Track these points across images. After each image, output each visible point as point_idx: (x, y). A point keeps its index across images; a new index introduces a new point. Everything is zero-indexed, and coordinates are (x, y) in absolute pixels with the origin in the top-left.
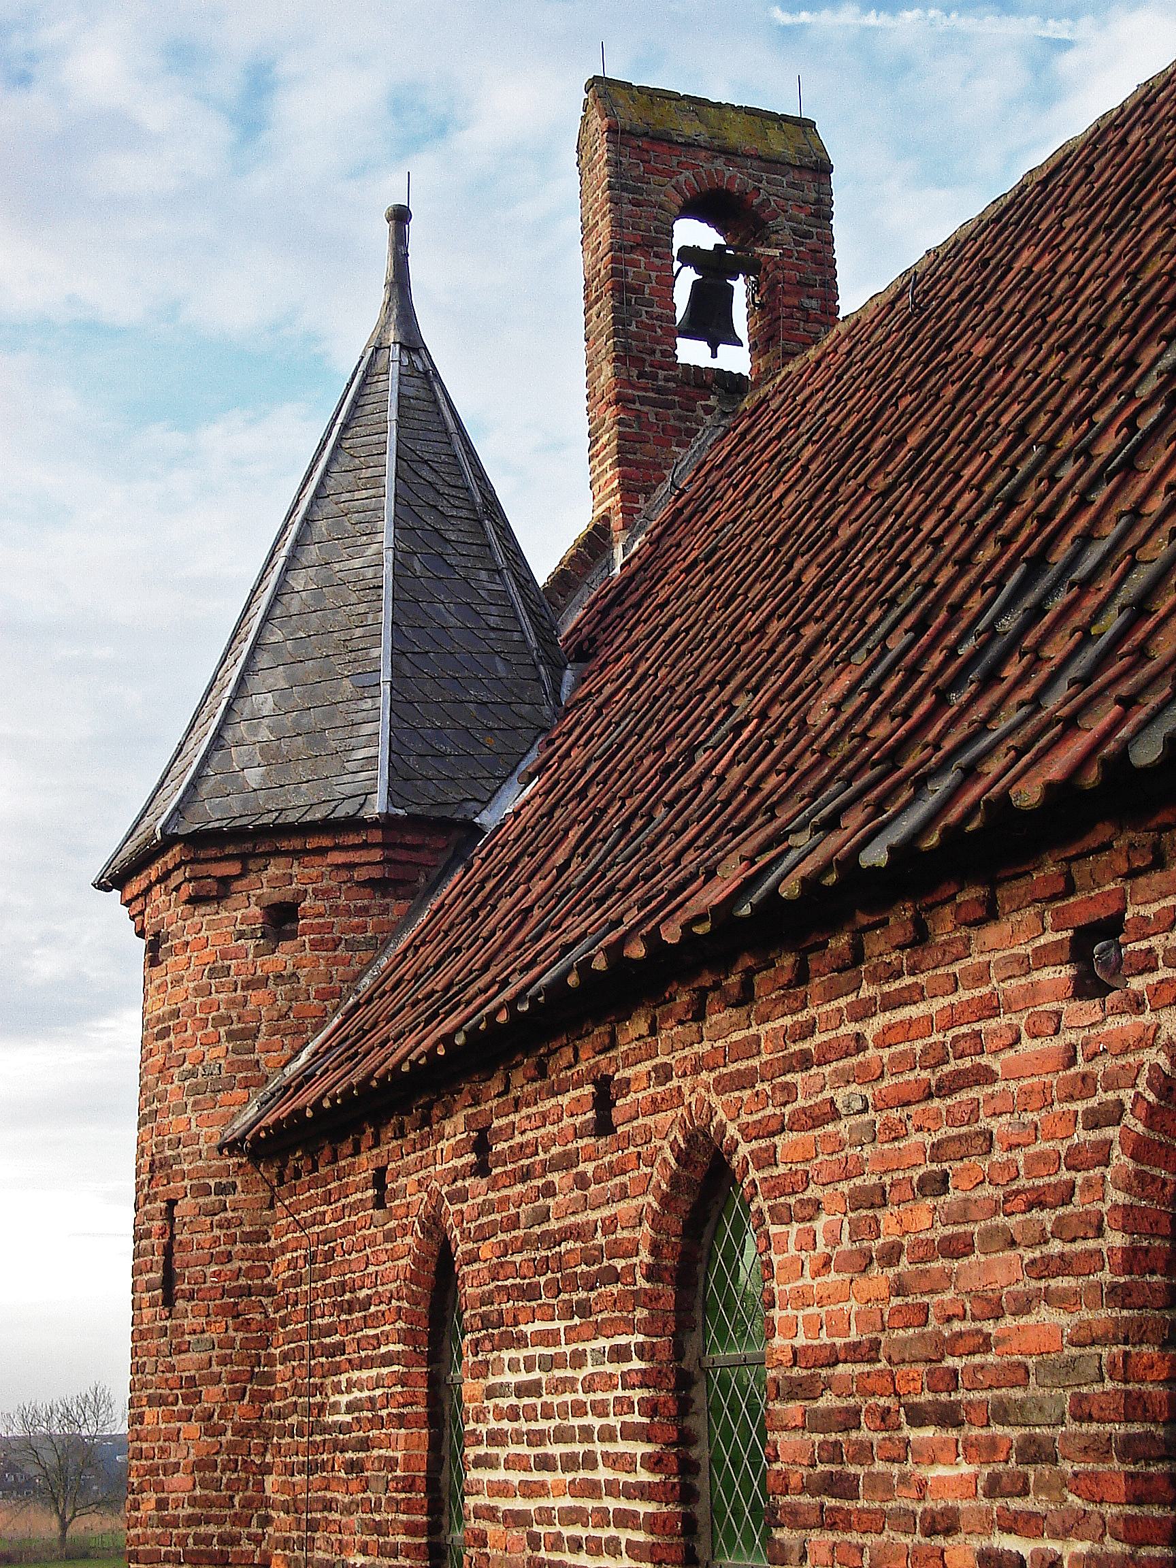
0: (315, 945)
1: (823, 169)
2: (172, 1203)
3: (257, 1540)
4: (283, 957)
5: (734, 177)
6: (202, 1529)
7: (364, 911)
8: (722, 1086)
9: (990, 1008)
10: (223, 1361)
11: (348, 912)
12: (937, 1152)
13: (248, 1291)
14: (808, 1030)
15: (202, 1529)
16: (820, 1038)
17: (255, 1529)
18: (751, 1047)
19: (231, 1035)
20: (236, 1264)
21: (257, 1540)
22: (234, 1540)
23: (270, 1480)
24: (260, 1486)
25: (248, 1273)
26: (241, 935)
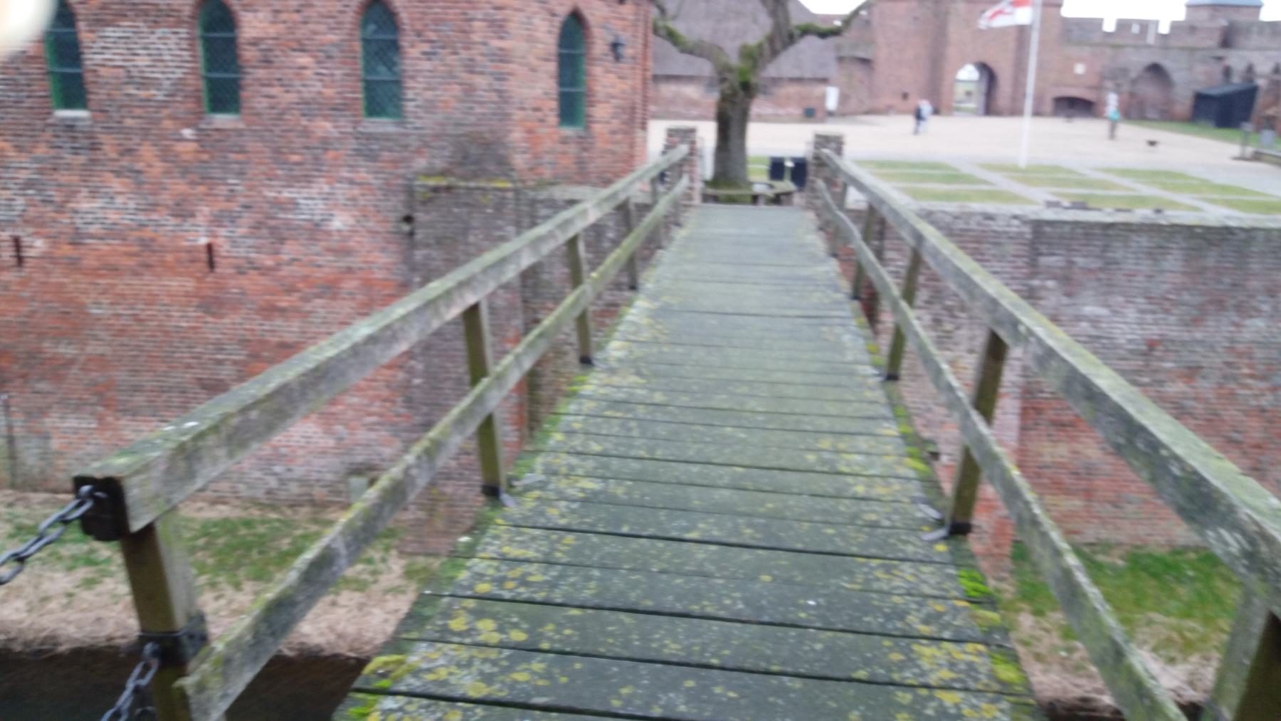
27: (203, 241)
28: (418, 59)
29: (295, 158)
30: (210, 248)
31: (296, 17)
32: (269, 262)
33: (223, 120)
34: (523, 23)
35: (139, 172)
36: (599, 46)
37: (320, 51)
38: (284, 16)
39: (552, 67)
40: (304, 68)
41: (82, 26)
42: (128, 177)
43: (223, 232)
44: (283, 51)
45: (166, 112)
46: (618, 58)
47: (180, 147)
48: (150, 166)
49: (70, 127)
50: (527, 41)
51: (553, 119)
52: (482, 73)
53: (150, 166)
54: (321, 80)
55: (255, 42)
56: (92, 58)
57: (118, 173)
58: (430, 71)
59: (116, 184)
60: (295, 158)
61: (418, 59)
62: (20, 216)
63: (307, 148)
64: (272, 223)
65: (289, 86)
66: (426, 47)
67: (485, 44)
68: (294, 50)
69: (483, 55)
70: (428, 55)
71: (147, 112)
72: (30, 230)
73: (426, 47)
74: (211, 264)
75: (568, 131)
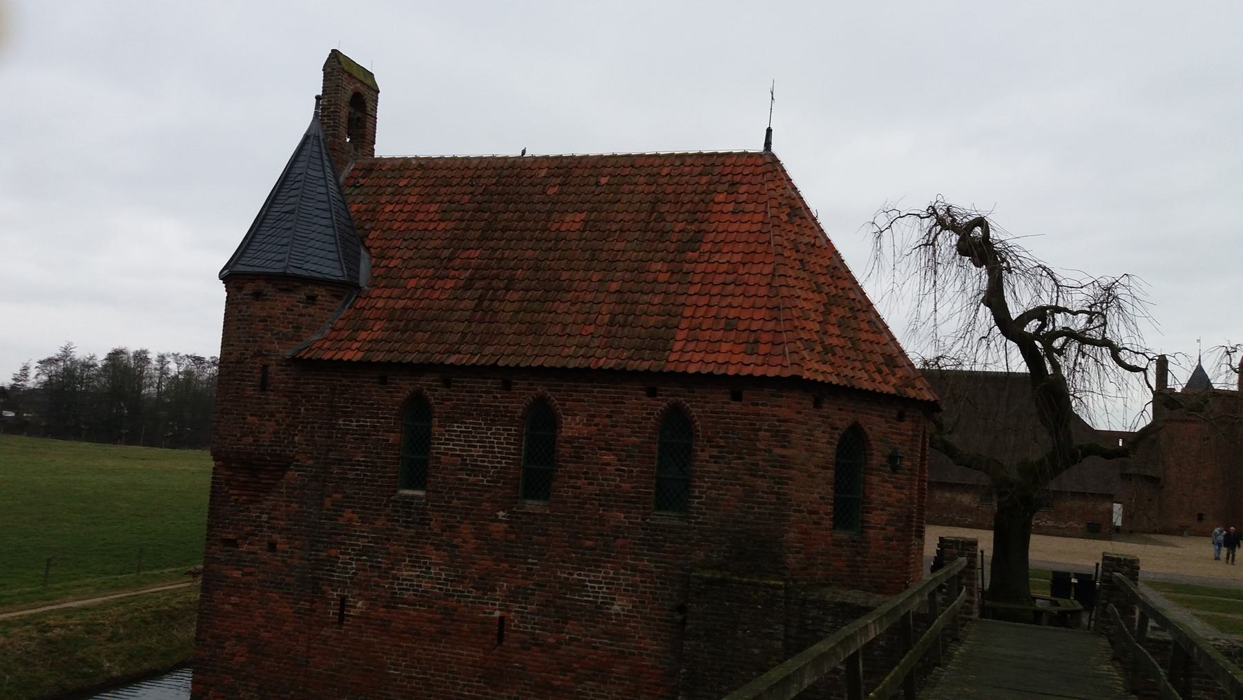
0: (320, 309)
1: (378, 92)
2: (265, 367)
3: (292, 451)
4: (311, 310)
5: (362, 89)
6: (274, 448)
7: (332, 302)
8: (549, 390)
9: (626, 394)
10: (284, 408)
11: (328, 302)
12: (611, 412)
13: (291, 392)
14: (578, 387)
15: (274, 448)
16: (581, 388)
17: (291, 449)
18: (562, 386)
19: (293, 327)
20: (290, 385)
21: (292, 451)
22: (285, 451)
23: (296, 438)
24: (293, 439)
25: (294, 387)
26: (299, 302)
27: (497, 614)
28: (707, 461)
29: (589, 543)
30: (501, 619)
31: (607, 421)
32: (551, 640)
33: (533, 505)
34: (804, 434)
35: (456, 546)
36: (877, 459)
37: (622, 450)
38: (597, 420)
39: (830, 474)
40: (609, 464)
41: (435, 421)
42: (445, 550)
43: (515, 607)
44: (592, 449)
45: (487, 495)
46: (895, 469)
47: (493, 527)
48: (464, 542)
49: (408, 503)
50: (807, 450)
51: (828, 523)
52: (763, 476)
53: (464, 542)
54: (620, 476)
55: (569, 440)
56: (438, 447)
57: (438, 547)
58: (715, 473)
59: (434, 556)
60: (589, 543)
61: (707, 461)
62: (350, 578)
63: (599, 535)
64: (559, 602)
65: (592, 479)
66: (715, 452)
67: (769, 451)
68: (600, 449)
69: (764, 460)
70: (716, 459)
71: (470, 495)
72: (356, 592)
73: (715, 452)
74: (500, 637)
75: (842, 535)
